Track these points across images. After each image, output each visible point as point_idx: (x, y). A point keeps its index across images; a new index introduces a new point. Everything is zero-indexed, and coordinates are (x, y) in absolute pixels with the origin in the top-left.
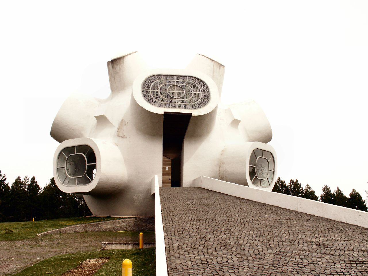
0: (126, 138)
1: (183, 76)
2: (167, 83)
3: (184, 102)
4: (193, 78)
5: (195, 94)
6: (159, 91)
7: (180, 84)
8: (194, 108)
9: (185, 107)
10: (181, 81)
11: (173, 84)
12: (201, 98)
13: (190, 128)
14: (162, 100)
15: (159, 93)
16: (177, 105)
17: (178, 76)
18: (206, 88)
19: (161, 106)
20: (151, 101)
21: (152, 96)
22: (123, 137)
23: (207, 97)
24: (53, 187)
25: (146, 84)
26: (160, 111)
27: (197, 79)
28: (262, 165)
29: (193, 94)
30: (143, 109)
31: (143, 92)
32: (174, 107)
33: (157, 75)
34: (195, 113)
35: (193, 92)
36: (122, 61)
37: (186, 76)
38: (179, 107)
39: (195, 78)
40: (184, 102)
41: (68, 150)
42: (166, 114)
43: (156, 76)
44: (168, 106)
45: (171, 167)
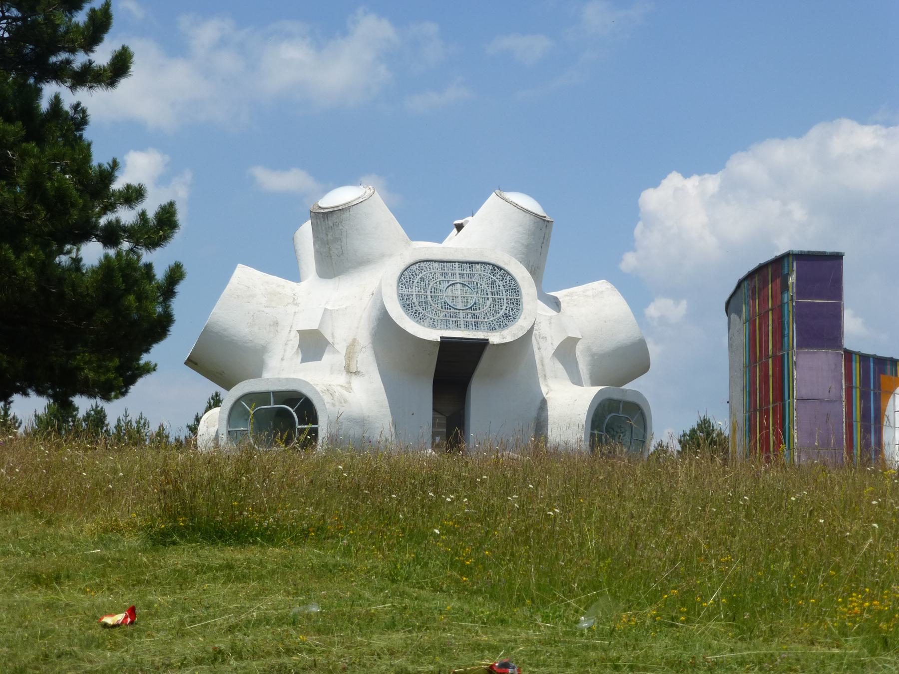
0: (363, 375)
1: (471, 263)
2: (442, 278)
4: (491, 267)
5: (494, 300)
6: (429, 293)
7: (466, 280)
8: (492, 329)
9: (477, 325)
10: (468, 272)
12: (504, 308)
15: (429, 297)
16: (462, 323)
17: (463, 262)
19: (433, 326)
20: (417, 316)
21: (417, 304)
22: (357, 373)
23: (516, 304)
24: (245, 464)
26: (435, 335)
27: (498, 267)
28: (620, 427)
29: (491, 300)
31: (402, 297)
33: (423, 261)
34: (495, 338)
35: (490, 296)
36: (346, 215)
37: (478, 263)
39: (493, 265)
40: (475, 316)
42: (446, 344)
43: (422, 264)
45: (445, 430)
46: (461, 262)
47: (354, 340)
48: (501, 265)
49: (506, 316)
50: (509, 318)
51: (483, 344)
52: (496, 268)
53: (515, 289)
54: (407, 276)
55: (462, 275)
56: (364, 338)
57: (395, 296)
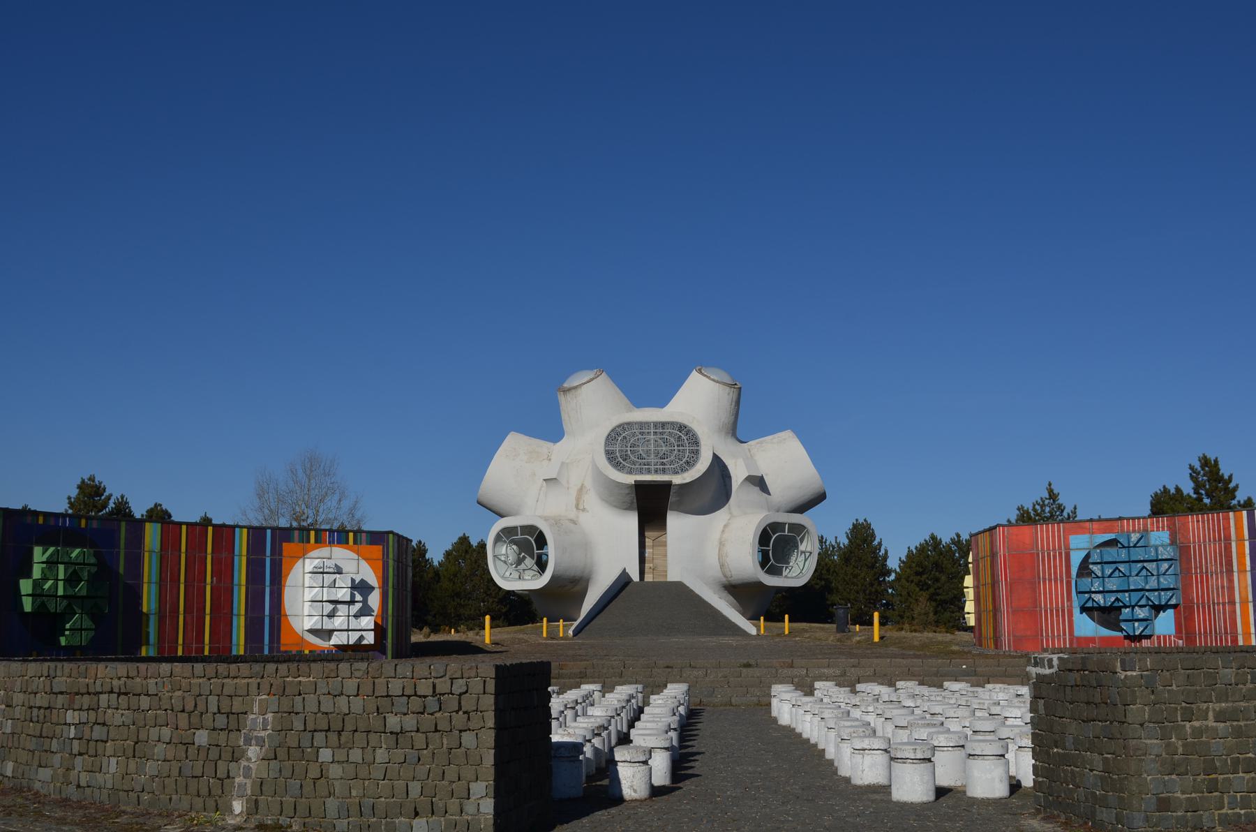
3: (663, 464)
8: (677, 473)
9: (664, 471)
11: (648, 437)
13: (672, 499)
14: (634, 463)
18: (695, 441)
19: (630, 473)
20: (617, 465)
22: (584, 510)
25: (612, 437)
26: (630, 479)
30: (607, 478)
31: (608, 453)
32: (649, 472)
34: (677, 480)
36: (579, 391)
38: (656, 471)
40: (663, 464)
41: (508, 533)
44: (642, 473)
46: (656, 424)
47: (582, 487)
48: (686, 423)
49: (688, 463)
50: (690, 464)
51: (668, 485)
52: (682, 427)
53: (697, 443)
54: (614, 436)
55: (655, 433)
56: (589, 483)
57: (603, 451)
